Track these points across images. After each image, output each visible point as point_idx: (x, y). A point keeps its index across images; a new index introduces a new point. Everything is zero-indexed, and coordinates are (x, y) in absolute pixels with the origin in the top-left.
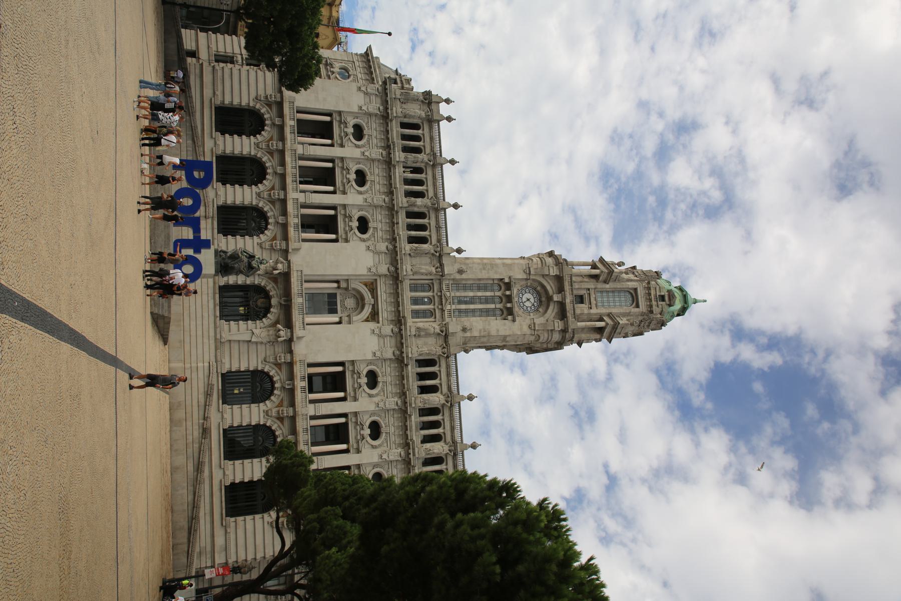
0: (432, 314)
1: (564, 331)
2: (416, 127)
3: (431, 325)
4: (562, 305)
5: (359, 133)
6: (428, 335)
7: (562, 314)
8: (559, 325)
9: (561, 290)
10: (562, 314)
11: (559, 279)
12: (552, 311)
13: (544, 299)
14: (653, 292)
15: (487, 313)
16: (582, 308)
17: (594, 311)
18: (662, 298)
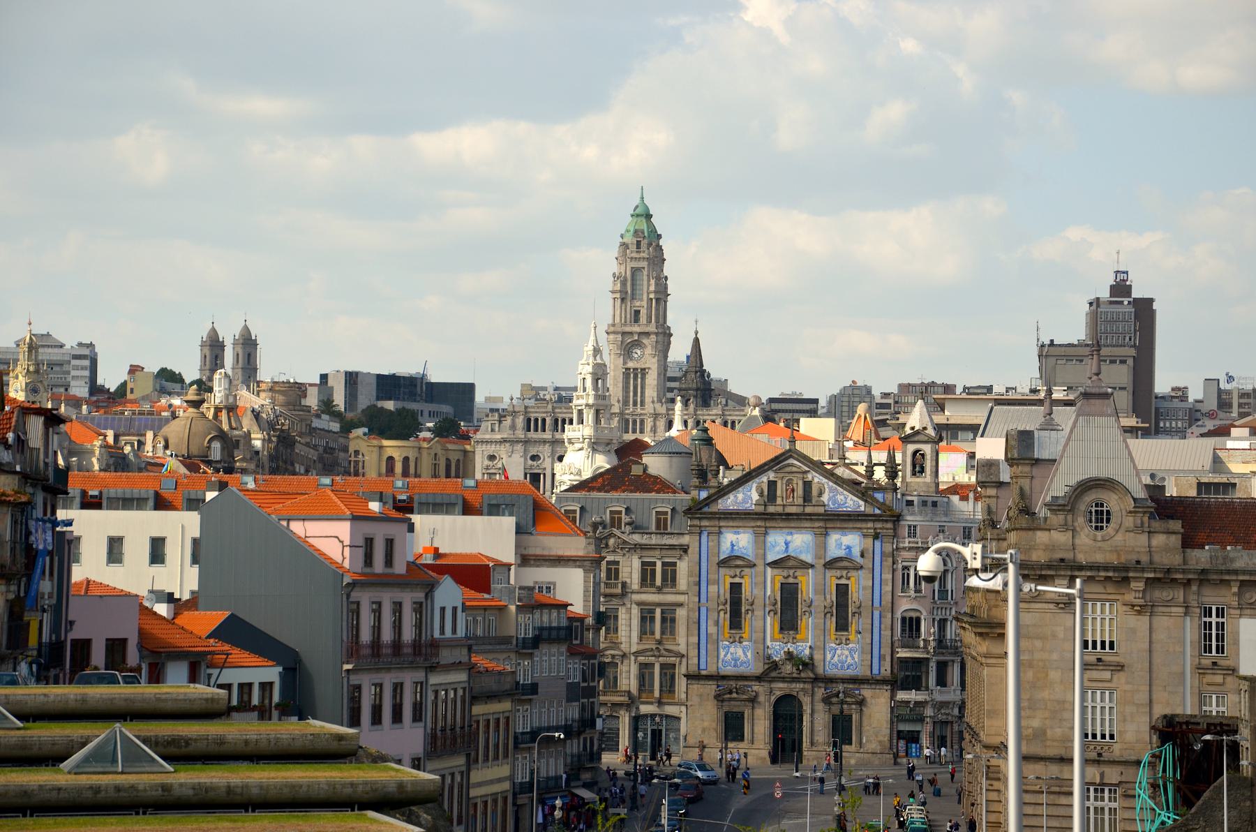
0: (642, 422)
1: (657, 334)
2: (529, 420)
3: (649, 423)
4: (640, 334)
5: (534, 458)
6: (655, 425)
7: (647, 334)
8: (653, 337)
9: (631, 333)
10: (647, 334)
11: (624, 334)
12: (645, 341)
13: (637, 344)
14: (634, 255)
15: (643, 388)
16: (643, 319)
17: (645, 303)
18: (638, 243)
